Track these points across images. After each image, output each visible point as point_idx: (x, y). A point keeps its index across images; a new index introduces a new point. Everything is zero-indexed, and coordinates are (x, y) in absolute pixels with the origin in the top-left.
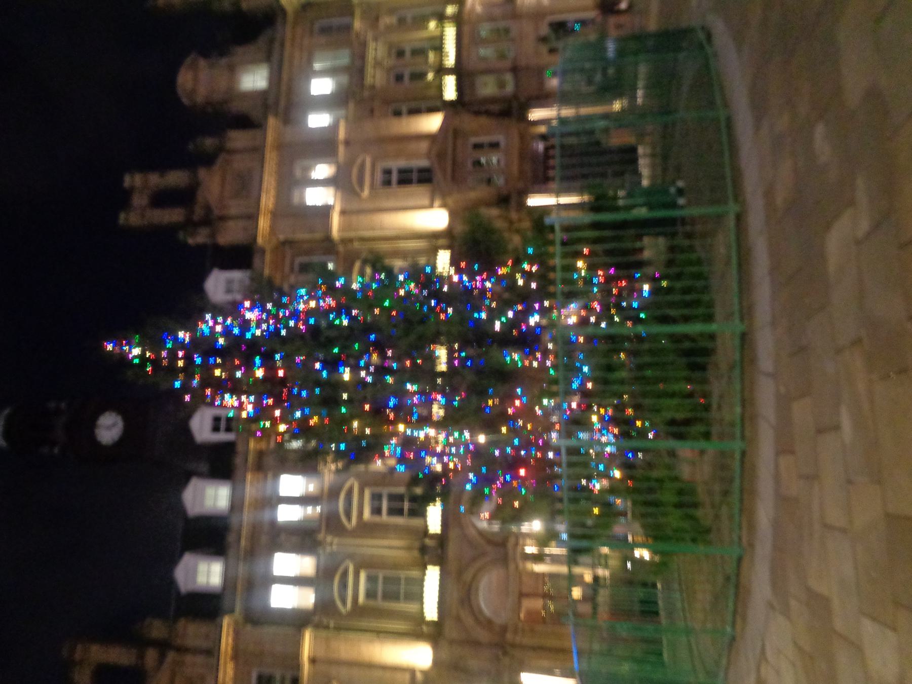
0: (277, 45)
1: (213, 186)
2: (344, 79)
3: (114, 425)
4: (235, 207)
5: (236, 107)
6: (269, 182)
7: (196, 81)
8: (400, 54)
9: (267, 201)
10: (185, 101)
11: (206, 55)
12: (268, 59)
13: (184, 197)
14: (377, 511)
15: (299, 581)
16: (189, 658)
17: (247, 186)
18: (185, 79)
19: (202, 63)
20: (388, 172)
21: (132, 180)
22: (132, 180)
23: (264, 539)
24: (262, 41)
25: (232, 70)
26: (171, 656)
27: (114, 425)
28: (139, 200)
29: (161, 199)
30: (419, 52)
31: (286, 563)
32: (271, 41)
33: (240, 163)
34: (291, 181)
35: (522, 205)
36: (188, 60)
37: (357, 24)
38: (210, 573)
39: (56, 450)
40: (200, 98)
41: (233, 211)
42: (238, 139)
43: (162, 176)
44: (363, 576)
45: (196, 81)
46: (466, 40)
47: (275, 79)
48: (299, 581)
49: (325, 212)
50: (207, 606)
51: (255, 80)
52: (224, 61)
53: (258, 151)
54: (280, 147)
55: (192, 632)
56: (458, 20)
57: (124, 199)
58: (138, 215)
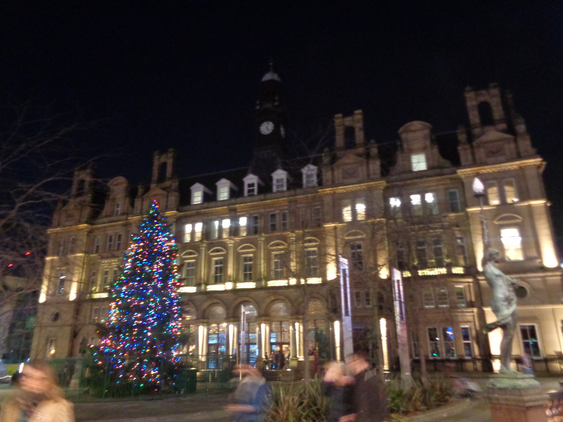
0: (438, 171)
1: (349, 159)
2: (420, 213)
3: (268, 130)
4: (338, 173)
5: (400, 157)
6: (351, 188)
7: (417, 131)
8: (437, 242)
9: (340, 189)
10: (401, 129)
11: (433, 131)
12: (430, 168)
13: (350, 144)
14: (217, 262)
15: (193, 233)
16: (165, 199)
17: (350, 176)
18: (416, 124)
19: (427, 132)
20: (359, 247)
21: (358, 114)
22: (358, 114)
23: (205, 218)
24: (443, 161)
25: (423, 150)
26: (165, 193)
27: (268, 130)
28: (348, 121)
29: (350, 132)
30: (438, 252)
31: (199, 227)
32: (441, 167)
33: (362, 171)
34: (353, 198)
35: (381, 316)
36: (427, 124)
37: (452, 215)
38: (197, 198)
39: (258, 107)
40: (404, 136)
41: (336, 173)
42: (376, 166)
43: (361, 129)
44: (194, 261)
45: (417, 131)
46: (435, 281)
47: (421, 175)
48: (193, 233)
49: (339, 217)
50: (185, 199)
51: (419, 163)
52: (428, 143)
53: (369, 178)
54: (370, 189)
55: (173, 198)
56: (450, 275)
57: (348, 113)
58: (340, 122)
